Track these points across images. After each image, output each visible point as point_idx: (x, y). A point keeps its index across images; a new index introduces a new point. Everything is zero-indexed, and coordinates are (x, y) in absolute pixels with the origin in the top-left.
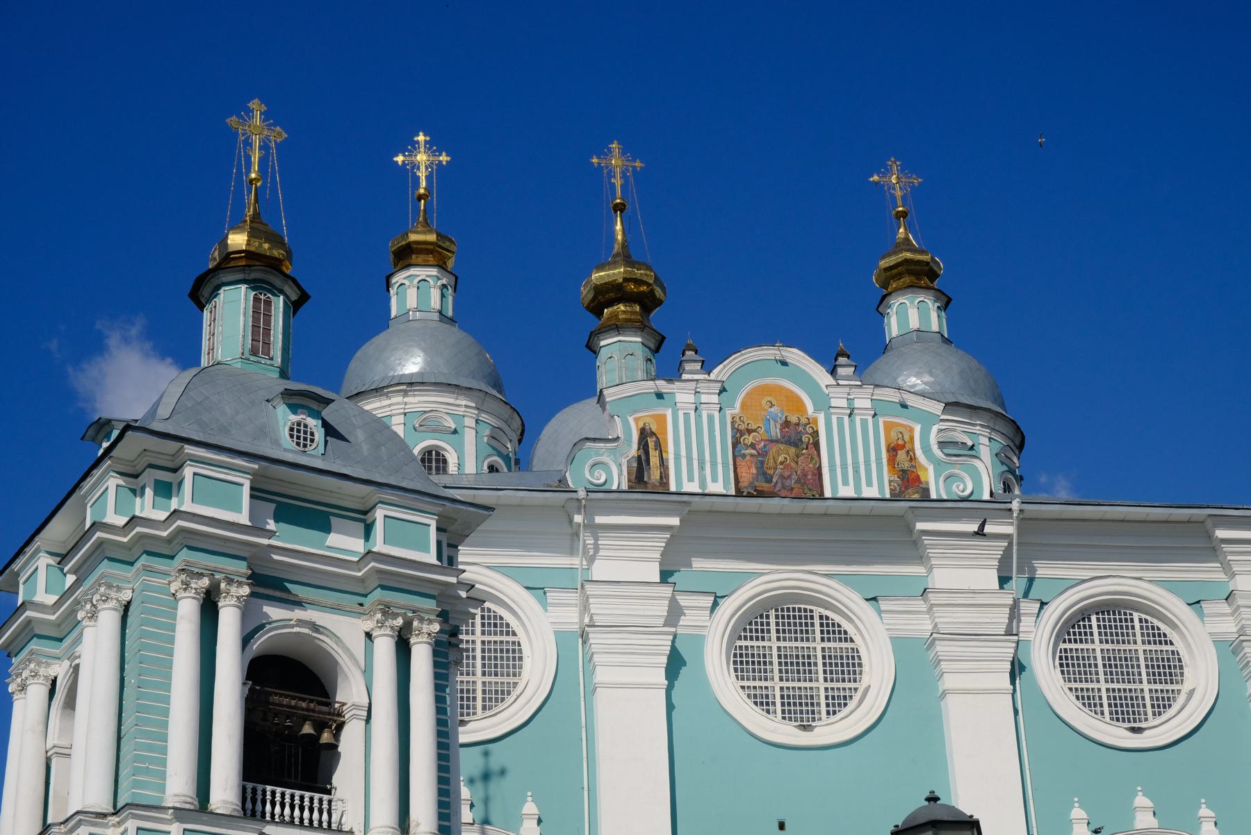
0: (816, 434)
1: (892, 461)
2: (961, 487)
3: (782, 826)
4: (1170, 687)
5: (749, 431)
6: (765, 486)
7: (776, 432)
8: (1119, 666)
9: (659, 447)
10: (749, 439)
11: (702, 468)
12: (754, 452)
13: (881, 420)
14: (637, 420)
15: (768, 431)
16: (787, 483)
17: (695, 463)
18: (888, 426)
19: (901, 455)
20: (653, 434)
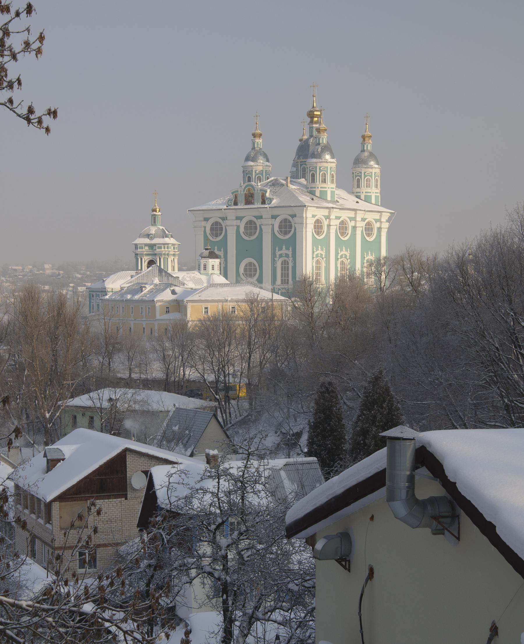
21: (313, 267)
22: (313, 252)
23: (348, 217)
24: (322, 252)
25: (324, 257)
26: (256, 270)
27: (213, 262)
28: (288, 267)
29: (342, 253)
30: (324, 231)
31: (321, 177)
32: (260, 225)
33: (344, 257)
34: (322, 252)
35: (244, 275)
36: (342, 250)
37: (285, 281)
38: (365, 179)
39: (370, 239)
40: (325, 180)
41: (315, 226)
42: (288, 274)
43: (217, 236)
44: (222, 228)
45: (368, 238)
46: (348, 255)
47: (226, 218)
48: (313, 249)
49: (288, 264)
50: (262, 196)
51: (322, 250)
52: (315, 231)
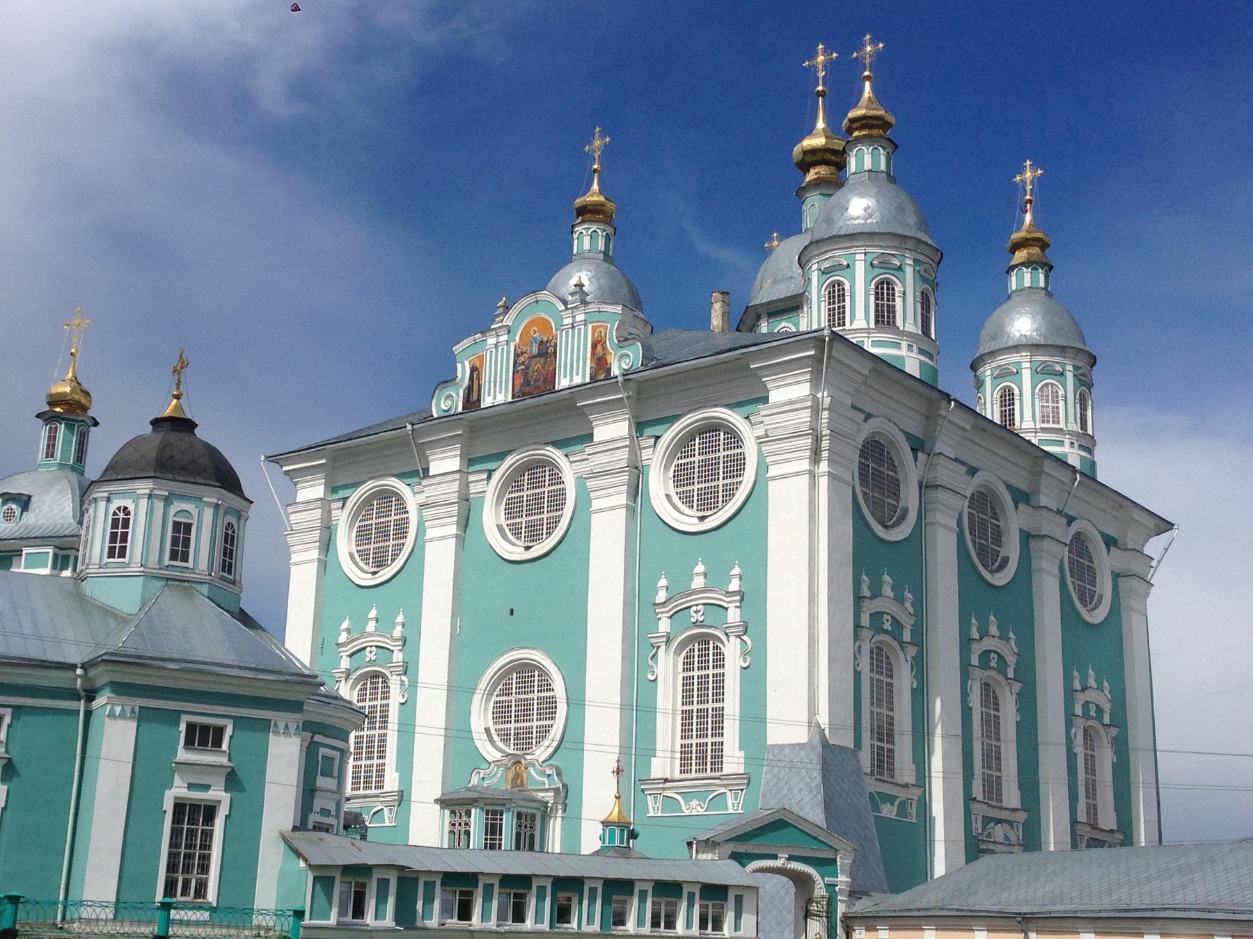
0: (556, 344)
1: (593, 354)
2: (627, 361)
3: (512, 612)
4: (735, 480)
5: (522, 353)
6: (527, 389)
7: (535, 350)
8: (709, 471)
9: (479, 378)
10: (522, 359)
11: (495, 386)
12: (523, 367)
13: (590, 327)
14: (470, 362)
15: (531, 351)
16: (538, 384)
17: (492, 384)
18: (594, 329)
19: (599, 347)
20: (477, 369)
21: (857, 675)
22: (858, 599)
23: (1010, 487)
24: (894, 609)
25: (907, 636)
26: (549, 708)
27: (183, 497)
28: (719, 679)
29: (988, 644)
30: (905, 511)
31: (872, 298)
32: (581, 481)
33: (993, 664)
34: (894, 609)
35: (492, 741)
36: (984, 634)
37: (702, 759)
38: (1037, 391)
39: (1098, 616)
40: (892, 310)
41: (863, 467)
42: (719, 715)
43: (380, 564)
44: (406, 522)
45: (1083, 611)
46: (1011, 660)
47: (426, 470)
48: (857, 583)
49: (720, 661)
50: (594, 346)
51: (899, 599)
52: (865, 494)
